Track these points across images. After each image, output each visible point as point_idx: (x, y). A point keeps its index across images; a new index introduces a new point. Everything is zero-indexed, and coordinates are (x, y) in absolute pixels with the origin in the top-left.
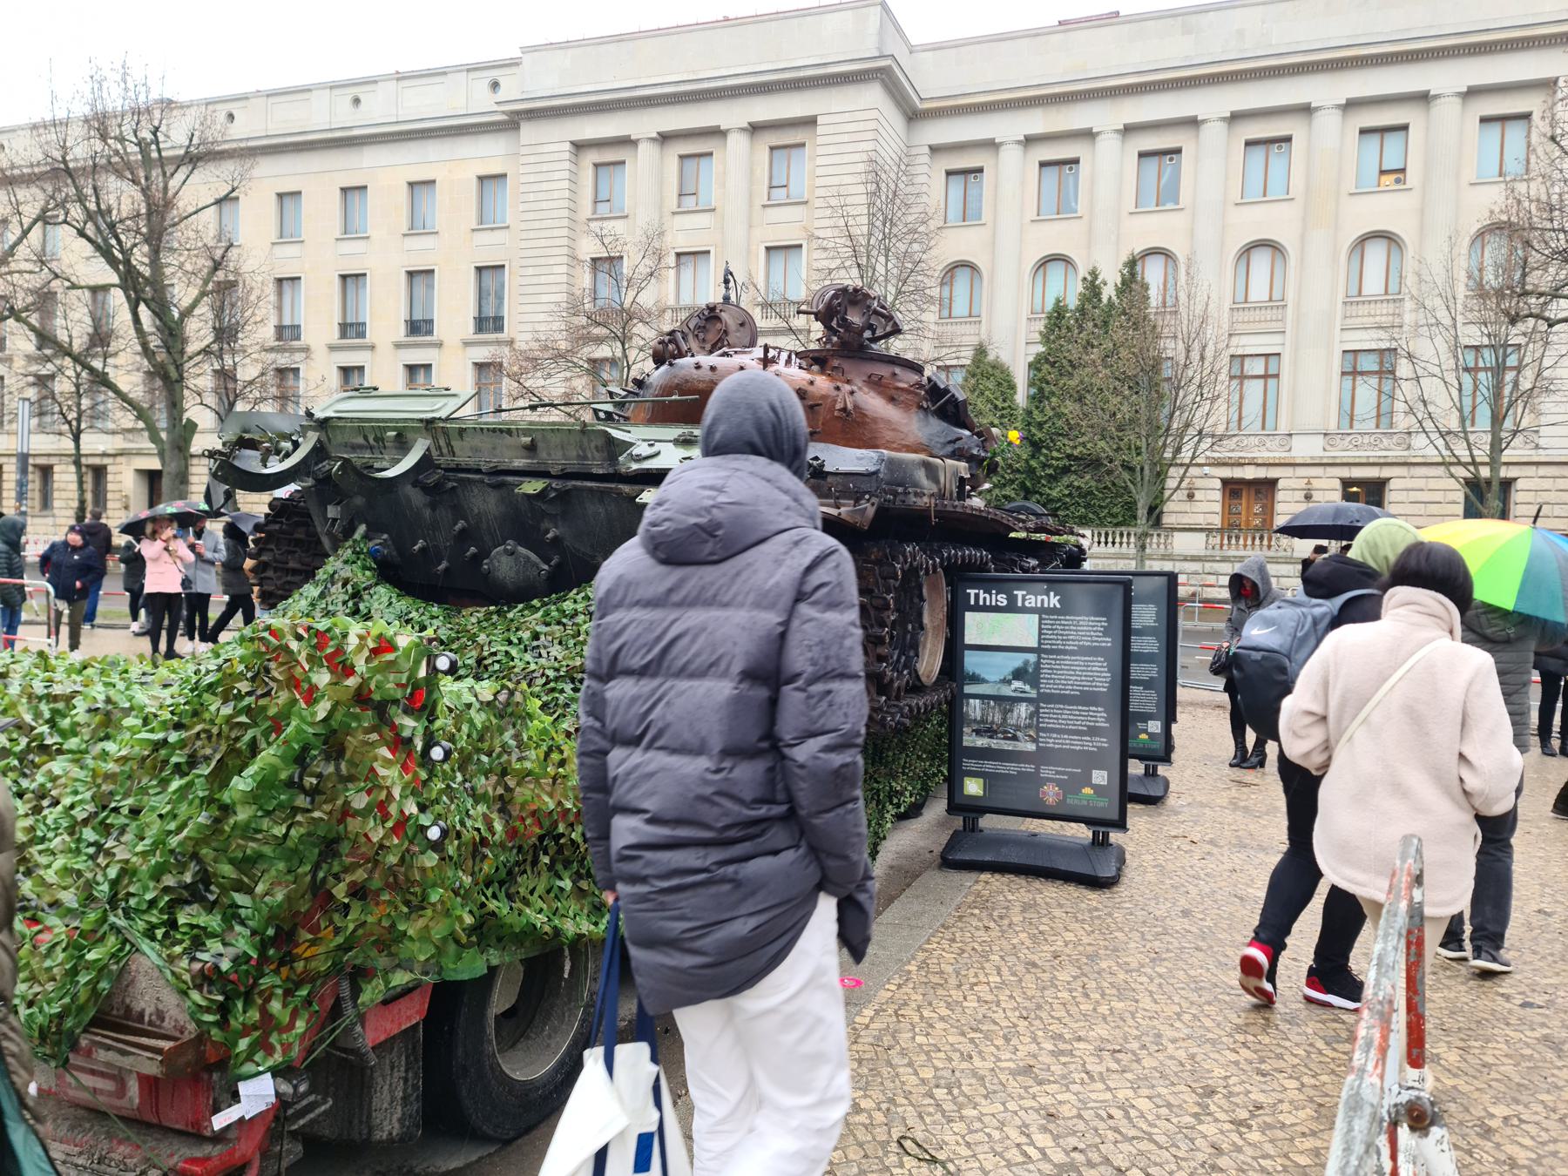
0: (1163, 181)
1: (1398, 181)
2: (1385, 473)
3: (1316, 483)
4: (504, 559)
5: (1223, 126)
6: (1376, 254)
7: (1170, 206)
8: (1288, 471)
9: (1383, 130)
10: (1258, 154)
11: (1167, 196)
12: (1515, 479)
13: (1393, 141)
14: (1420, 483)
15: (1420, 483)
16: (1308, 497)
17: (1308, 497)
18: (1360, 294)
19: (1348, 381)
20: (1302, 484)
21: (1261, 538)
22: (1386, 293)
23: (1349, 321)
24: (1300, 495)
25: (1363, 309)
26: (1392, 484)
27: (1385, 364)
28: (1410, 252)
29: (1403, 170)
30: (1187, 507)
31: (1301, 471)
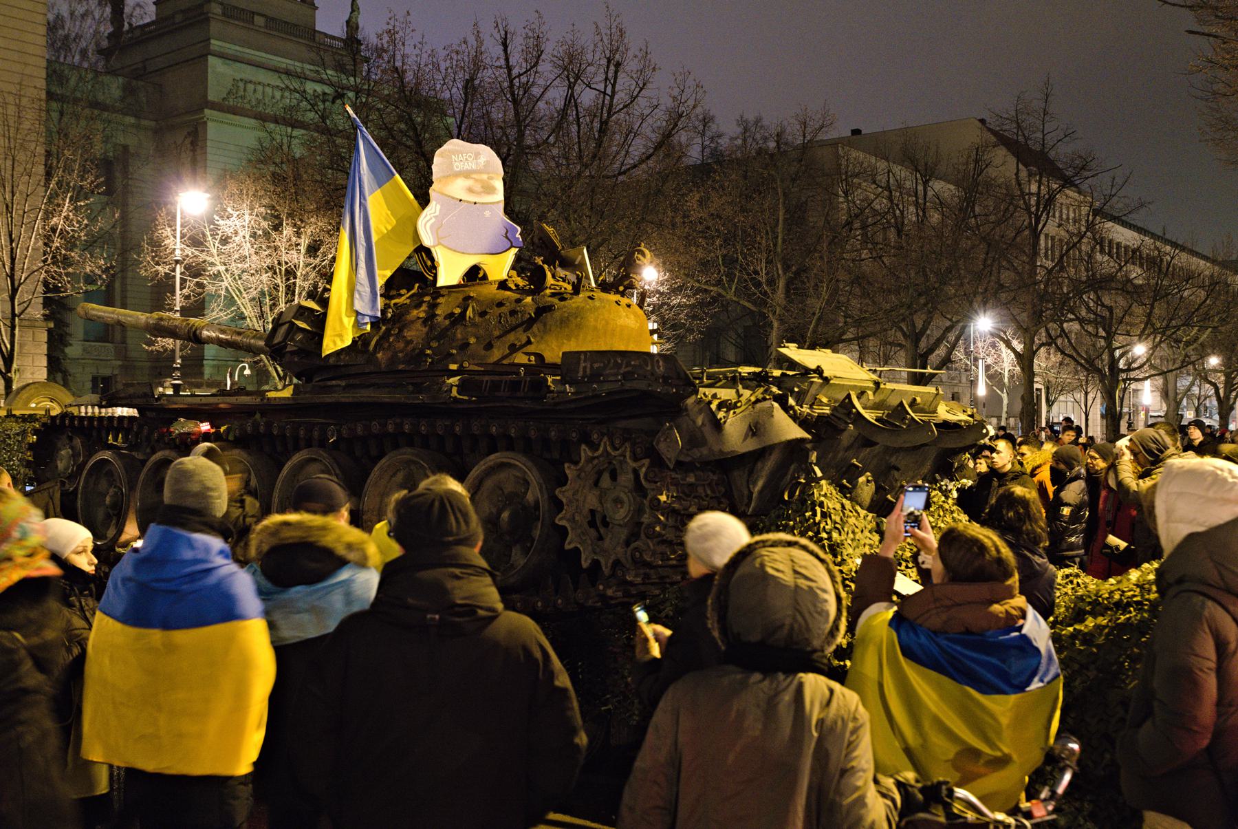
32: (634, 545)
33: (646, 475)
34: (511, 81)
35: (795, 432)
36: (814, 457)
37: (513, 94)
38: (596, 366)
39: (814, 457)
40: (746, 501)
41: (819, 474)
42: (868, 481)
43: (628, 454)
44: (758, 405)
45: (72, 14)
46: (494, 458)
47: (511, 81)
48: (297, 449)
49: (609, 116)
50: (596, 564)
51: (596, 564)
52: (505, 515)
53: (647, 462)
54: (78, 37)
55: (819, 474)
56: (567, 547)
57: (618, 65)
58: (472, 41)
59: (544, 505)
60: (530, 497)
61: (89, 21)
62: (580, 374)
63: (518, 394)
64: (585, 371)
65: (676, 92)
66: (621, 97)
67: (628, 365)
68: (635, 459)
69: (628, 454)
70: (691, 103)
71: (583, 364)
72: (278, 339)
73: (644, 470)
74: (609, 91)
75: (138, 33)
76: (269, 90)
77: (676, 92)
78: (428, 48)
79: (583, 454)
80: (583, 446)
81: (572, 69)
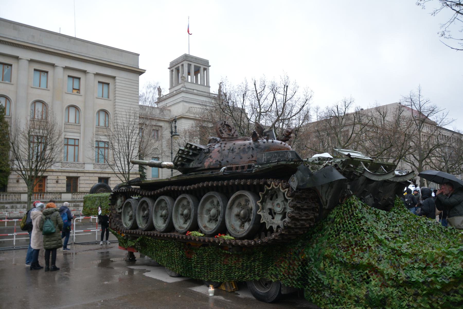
0: (5, 73)
1: (78, 92)
2: (79, 175)
3: (60, 178)
4: (370, 199)
5: (27, 62)
6: (72, 111)
7: (7, 82)
8: (51, 173)
9: (73, 77)
10: (38, 74)
11: (7, 78)
12: (110, 177)
13: (76, 81)
14: (88, 178)
15: (88, 178)
16: (57, 182)
17: (57, 182)
18: (68, 122)
19: (66, 147)
20: (56, 178)
21: (40, 195)
22: (75, 123)
23: (66, 129)
24: (54, 181)
25: (70, 127)
26: (81, 178)
27: (108, 145)
28: (111, 116)
29: (79, 90)
30: (16, 185)
31: (55, 174)
32: (284, 220)
33: (287, 194)
34: (257, 94)
35: (342, 177)
36: (349, 187)
37: (258, 98)
38: (268, 157)
39: (349, 187)
40: (325, 204)
41: (352, 193)
42: (371, 197)
43: (280, 188)
44: (326, 167)
45: (147, 93)
46: (237, 193)
47: (257, 94)
48: (180, 194)
49: (285, 102)
50: (271, 227)
51: (271, 227)
52: (242, 212)
53: (287, 190)
54: (148, 98)
55: (352, 193)
56: (262, 222)
57: (287, 87)
58: (245, 83)
59: (254, 208)
60: (250, 206)
61: (151, 93)
62: (263, 161)
63: (244, 170)
64: (265, 160)
65: (305, 93)
66: (289, 96)
67: (279, 156)
68: (283, 189)
69: (280, 188)
70: (310, 96)
71: (264, 157)
72: (176, 161)
73: (286, 193)
74: (285, 94)
75: (165, 97)
76: (198, 109)
77: (305, 93)
78: (232, 86)
79: (265, 189)
80: (265, 186)
81: (274, 90)
